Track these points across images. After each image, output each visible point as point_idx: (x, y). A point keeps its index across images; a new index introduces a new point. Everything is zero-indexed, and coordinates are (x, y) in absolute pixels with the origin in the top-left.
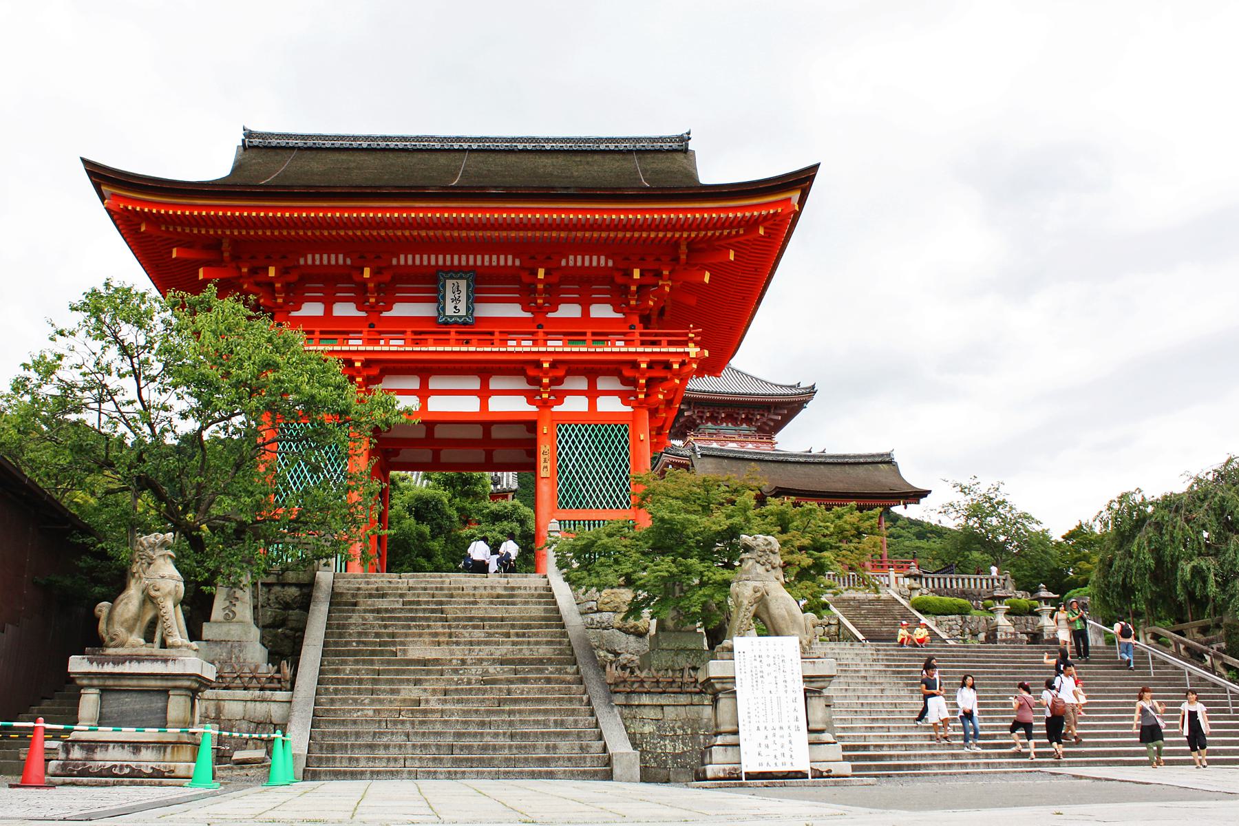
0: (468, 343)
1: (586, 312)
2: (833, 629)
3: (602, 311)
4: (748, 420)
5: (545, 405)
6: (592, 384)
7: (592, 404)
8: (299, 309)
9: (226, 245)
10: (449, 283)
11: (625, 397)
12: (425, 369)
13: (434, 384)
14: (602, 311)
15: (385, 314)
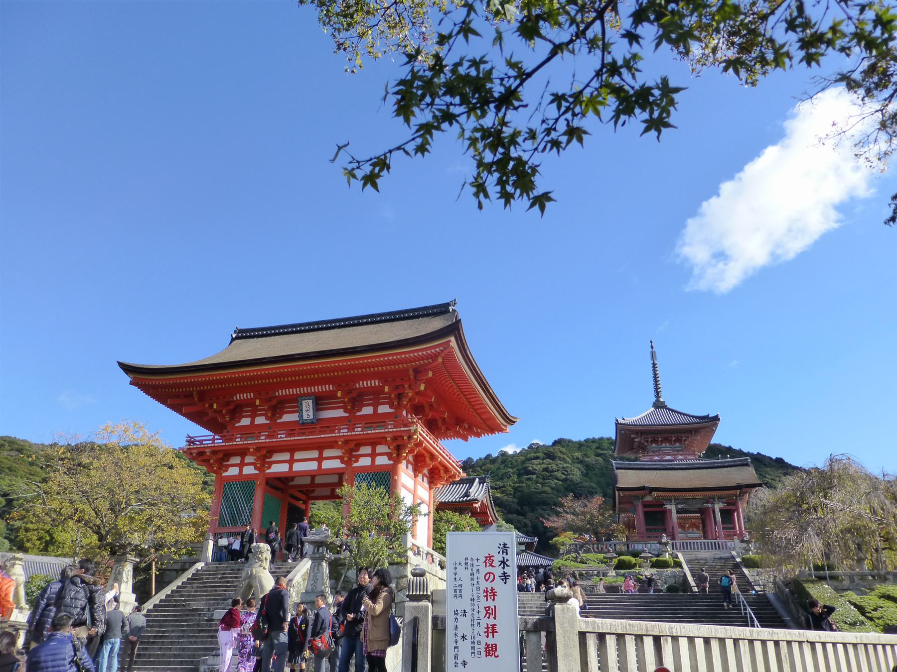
0: (303, 434)
1: (375, 410)
2: (681, 579)
3: (384, 409)
4: (679, 440)
5: (348, 463)
6: (374, 450)
7: (373, 461)
8: (239, 422)
9: (195, 394)
10: (304, 402)
11: (389, 456)
12: (292, 449)
13: (298, 455)
14: (384, 409)
15: (279, 421)
